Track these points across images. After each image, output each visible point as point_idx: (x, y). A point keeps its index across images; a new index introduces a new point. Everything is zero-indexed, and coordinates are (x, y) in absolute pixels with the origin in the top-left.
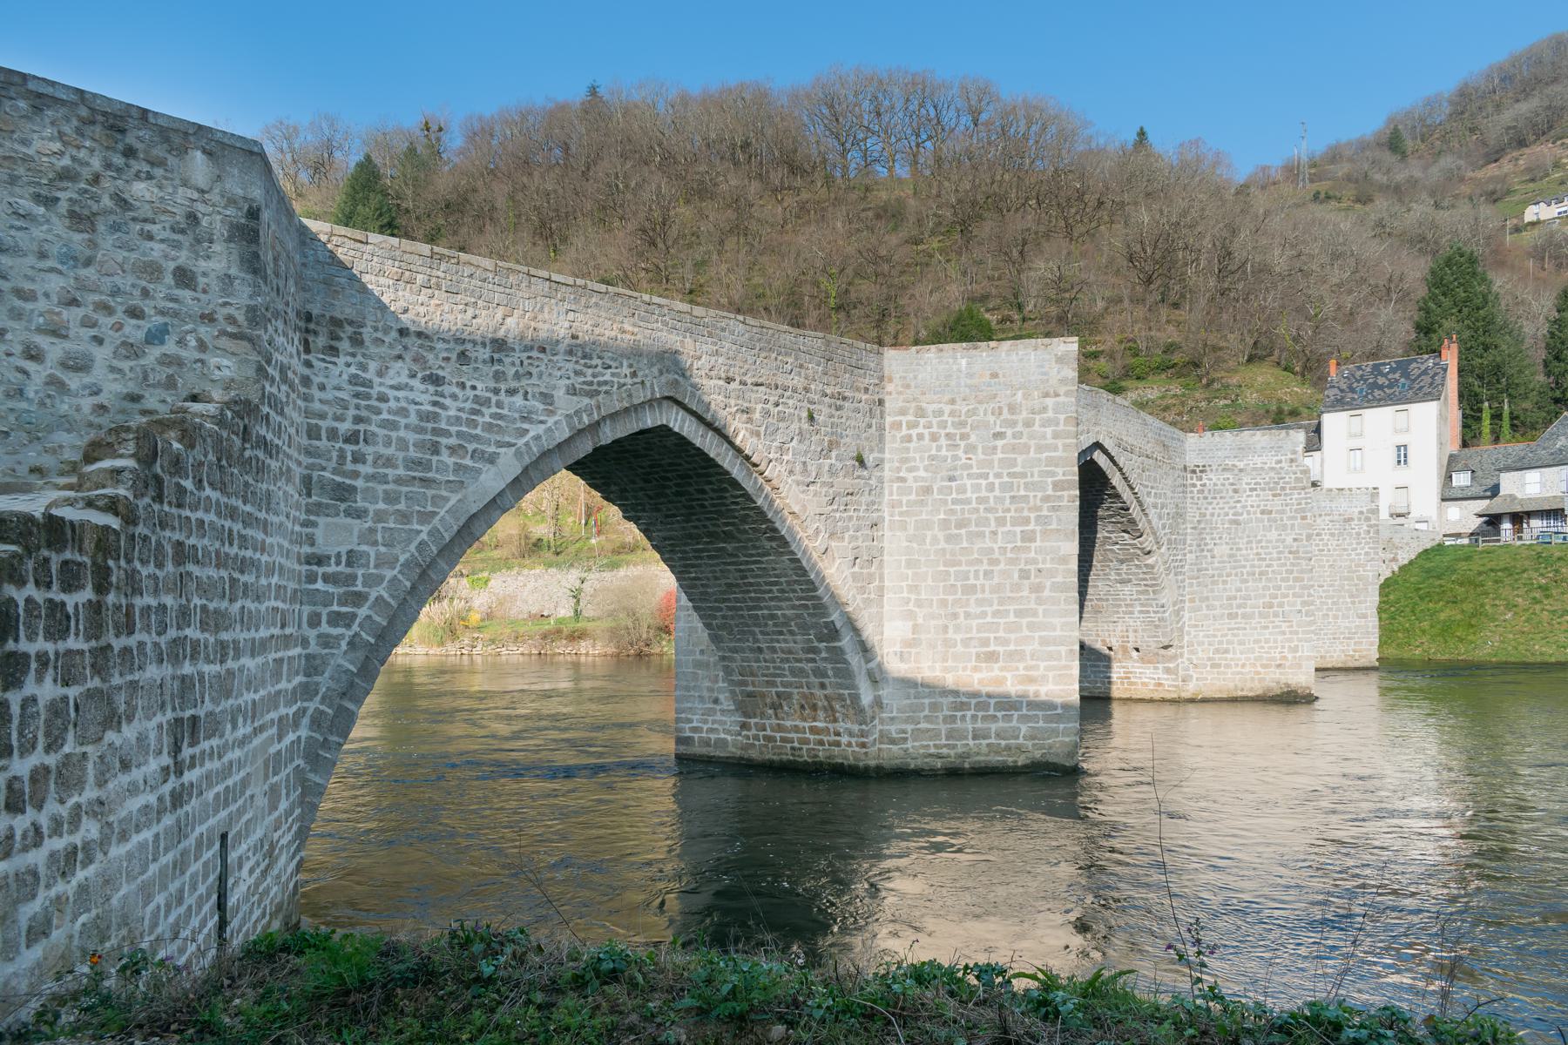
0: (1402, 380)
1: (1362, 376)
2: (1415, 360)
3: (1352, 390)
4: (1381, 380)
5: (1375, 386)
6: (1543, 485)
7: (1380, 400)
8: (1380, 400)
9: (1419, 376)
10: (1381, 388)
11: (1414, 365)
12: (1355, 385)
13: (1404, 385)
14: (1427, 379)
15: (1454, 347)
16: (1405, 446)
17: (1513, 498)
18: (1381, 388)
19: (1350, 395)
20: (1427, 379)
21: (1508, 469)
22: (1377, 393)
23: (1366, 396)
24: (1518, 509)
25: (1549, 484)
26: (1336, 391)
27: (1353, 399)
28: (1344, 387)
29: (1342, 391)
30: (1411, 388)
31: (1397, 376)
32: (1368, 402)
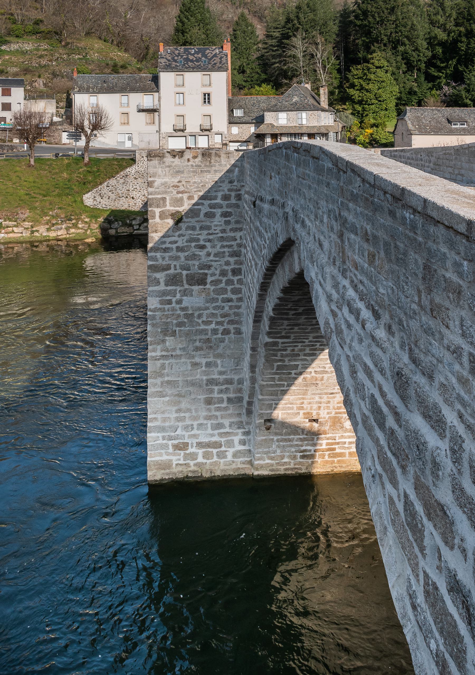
0: (203, 58)
1: (179, 53)
2: (208, 49)
3: (175, 61)
4: (191, 57)
5: (187, 60)
6: (288, 120)
7: (193, 68)
8: (193, 68)
9: (213, 57)
10: (192, 61)
11: (208, 51)
12: (176, 58)
13: (205, 61)
14: (217, 60)
15: (229, 44)
16: (209, 95)
17: (273, 126)
18: (192, 61)
19: (174, 63)
20: (217, 60)
21: (269, 110)
22: (190, 64)
23: (184, 65)
24: (277, 132)
25: (291, 120)
26: (165, 60)
27: (176, 65)
28: (170, 58)
29: (169, 60)
30: (210, 63)
31: (200, 55)
32: (187, 68)
